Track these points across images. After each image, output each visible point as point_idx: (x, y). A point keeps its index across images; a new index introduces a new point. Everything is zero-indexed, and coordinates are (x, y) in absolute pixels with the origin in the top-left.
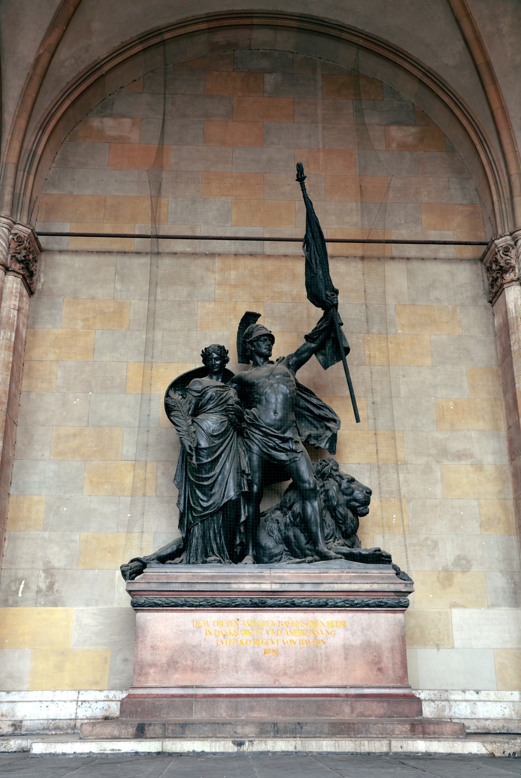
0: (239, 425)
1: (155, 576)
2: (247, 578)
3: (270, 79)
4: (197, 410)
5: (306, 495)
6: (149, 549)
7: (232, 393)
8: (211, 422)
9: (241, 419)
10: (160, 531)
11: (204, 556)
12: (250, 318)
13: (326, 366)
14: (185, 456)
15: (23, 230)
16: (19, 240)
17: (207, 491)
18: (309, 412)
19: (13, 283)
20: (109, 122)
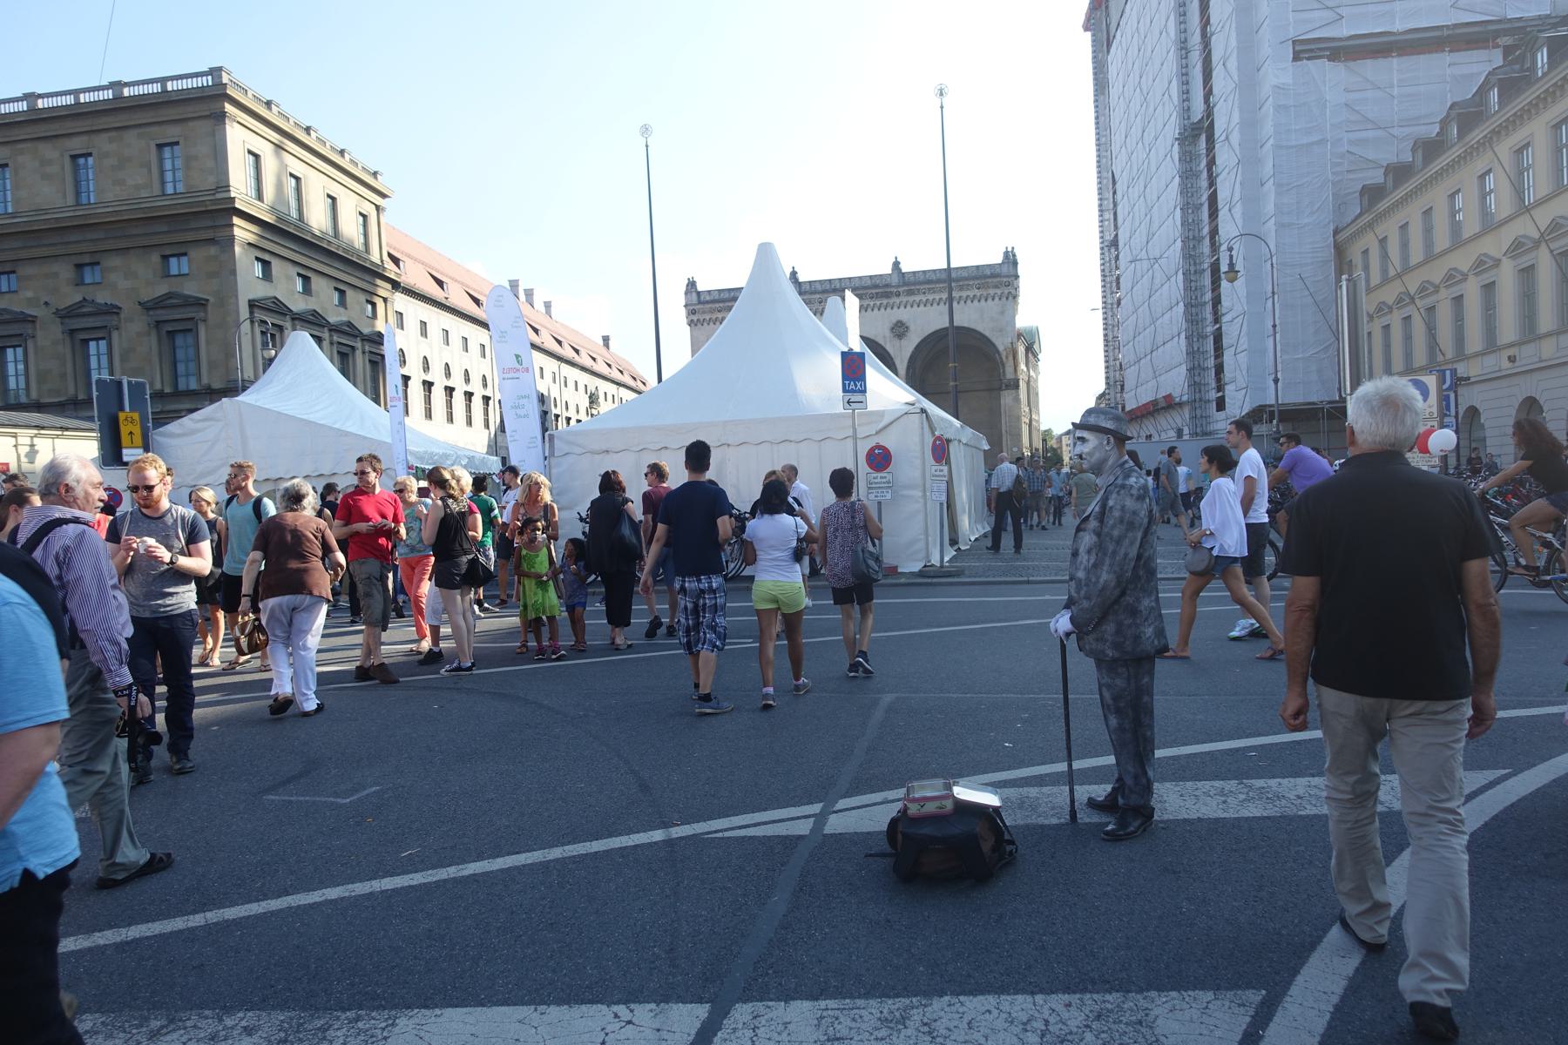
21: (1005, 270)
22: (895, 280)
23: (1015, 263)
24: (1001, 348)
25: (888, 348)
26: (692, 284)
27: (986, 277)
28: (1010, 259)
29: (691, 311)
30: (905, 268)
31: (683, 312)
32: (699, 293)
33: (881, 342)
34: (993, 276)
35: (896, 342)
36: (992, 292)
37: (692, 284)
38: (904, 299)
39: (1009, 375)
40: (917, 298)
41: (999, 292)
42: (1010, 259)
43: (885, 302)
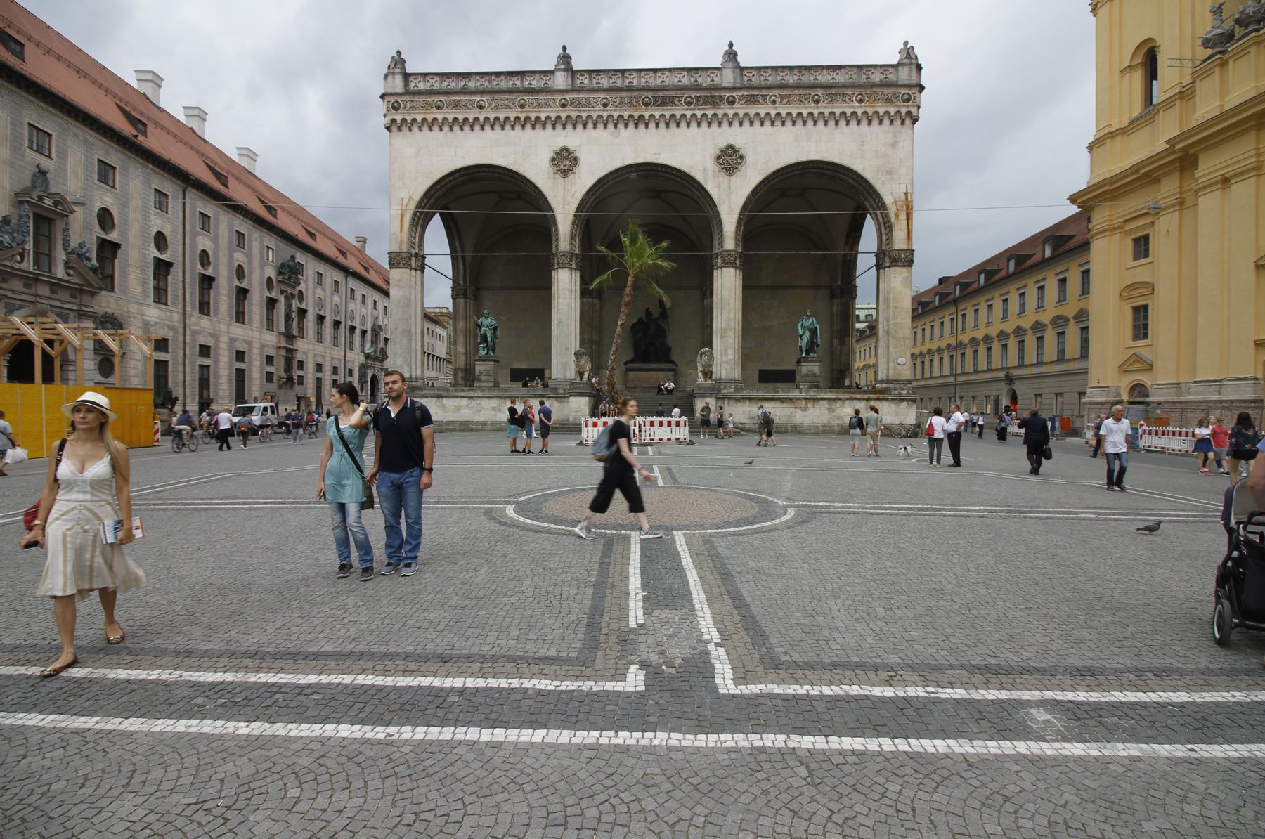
1: (630, 365)
2: (646, 366)
19: (597, 301)
21: (904, 75)
22: (728, 78)
23: (919, 68)
24: (888, 200)
25: (711, 187)
26: (398, 61)
27: (873, 85)
28: (909, 58)
30: (744, 61)
31: (381, 106)
32: (406, 76)
34: (884, 84)
35: (723, 178)
37: (398, 61)
39: (899, 243)
42: (909, 58)
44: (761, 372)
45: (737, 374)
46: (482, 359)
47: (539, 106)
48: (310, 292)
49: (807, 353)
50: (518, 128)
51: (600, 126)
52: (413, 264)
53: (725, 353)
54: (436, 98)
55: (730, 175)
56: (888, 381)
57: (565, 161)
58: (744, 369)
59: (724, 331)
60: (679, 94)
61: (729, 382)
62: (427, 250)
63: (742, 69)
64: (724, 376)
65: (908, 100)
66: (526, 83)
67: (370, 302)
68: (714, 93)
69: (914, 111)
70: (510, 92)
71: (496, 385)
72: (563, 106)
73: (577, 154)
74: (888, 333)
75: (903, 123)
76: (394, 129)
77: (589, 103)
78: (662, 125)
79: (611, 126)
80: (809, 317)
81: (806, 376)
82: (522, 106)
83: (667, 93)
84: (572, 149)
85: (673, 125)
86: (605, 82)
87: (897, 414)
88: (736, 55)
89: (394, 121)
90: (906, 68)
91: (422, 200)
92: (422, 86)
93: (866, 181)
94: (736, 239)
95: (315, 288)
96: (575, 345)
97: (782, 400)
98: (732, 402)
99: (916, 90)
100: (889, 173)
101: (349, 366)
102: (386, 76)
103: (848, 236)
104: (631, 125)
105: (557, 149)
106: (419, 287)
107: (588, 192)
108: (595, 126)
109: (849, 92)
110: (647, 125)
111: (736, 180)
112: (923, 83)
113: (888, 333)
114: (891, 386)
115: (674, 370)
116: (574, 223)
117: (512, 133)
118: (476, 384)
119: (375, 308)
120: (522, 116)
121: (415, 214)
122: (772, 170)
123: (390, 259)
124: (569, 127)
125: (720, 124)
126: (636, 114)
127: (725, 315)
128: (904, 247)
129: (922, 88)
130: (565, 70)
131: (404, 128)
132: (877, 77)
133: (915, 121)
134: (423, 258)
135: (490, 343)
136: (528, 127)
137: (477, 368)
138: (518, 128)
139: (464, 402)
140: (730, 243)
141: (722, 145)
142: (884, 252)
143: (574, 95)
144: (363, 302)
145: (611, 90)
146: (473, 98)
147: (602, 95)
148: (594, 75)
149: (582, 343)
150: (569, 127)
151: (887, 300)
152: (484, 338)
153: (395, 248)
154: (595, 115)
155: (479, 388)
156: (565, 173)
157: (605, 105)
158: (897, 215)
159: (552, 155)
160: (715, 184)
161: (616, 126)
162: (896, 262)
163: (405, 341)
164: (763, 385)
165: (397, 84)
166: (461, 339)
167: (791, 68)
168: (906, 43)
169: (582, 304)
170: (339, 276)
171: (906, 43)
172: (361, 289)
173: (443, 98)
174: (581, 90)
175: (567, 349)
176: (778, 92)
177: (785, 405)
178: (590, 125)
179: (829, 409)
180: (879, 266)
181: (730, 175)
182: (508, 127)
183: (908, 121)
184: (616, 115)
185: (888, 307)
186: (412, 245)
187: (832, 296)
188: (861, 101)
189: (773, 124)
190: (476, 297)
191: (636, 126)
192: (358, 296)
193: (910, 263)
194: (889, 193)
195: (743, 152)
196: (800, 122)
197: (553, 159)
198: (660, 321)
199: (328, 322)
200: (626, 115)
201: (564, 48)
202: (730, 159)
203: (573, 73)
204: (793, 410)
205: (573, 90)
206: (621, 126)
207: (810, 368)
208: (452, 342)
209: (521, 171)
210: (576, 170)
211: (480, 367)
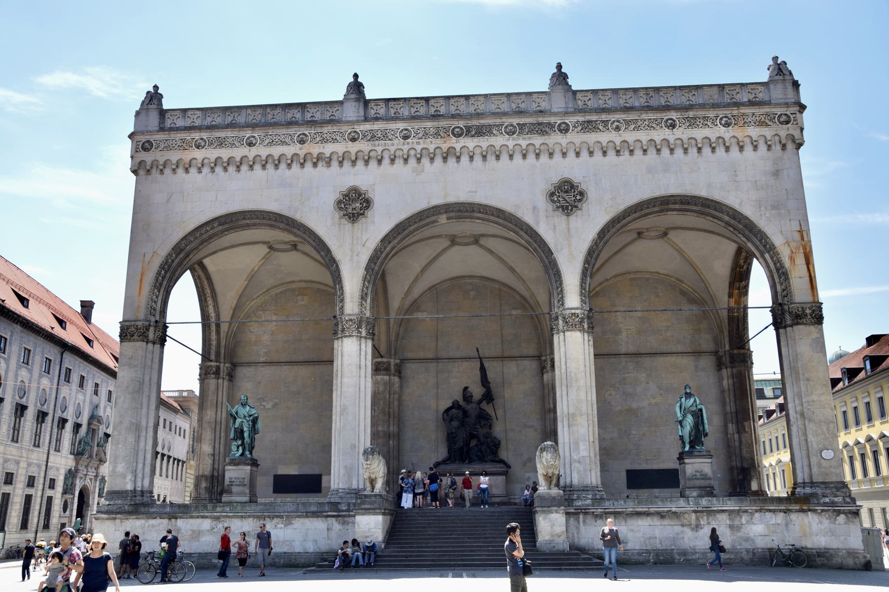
0: (463, 424)
3: (472, 293)
4: (451, 420)
5: (482, 444)
6: (440, 459)
7: (461, 413)
8: (455, 424)
9: (463, 422)
10: (442, 453)
11: (454, 461)
12: (466, 389)
13: (488, 403)
14: (448, 434)
15: (398, 361)
16: (396, 364)
17: (455, 444)
18: (485, 419)
19: (396, 379)
20: (420, 314)
23: (796, 85)
24: (778, 240)
25: (544, 230)
26: (154, 97)
29: (141, 143)
31: (127, 146)
32: (163, 113)
33: (528, 219)
35: (560, 219)
36: (754, 132)
37: (154, 97)
38: (576, 137)
39: (800, 294)
40: (604, 137)
41: (768, 132)
43: (537, 140)
44: (629, 472)
45: (594, 478)
46: (234, 462)
47: (324, 141)
48: (11, 375)
49: (692, 447)
50: (295, 167)
51: (399, 162)
52: (151, 335)
53: (576, 450)
54: (196, 135)
55: (568, 215)
56: (812, 484)
57: (354, 205)
58: (604, 468)
59: (571, 417)
60: (498, 121)
61: (585, 489)
62: (169, 319)
63: (575, 93)
64: (575, 481)
65: (787, 122)
66: (308, 116)
67: (89, 387)
68: (541, 120)
69: (796, 134)
70: (290, 124)
71: (253, 500)
72: (353, 140)
73: (370, 195)
74: (802, 415)
75: (784, 147)
76: (142, 172)
77: (385, 137)
78: (478, 159)
79: (412, 161)
80: (688, 395)
81: (693, 478)
82: (302, 142)
83: (482, 122)
84: (363, 188)
85: (491, 158)
86: (405, 112)
87: (832, 533)
88: (565, 77)
89: (141, 163)
90: (780, 86)
91: (169, 255)
92: (180, 123)
93: (746, 218)
94: (581, 294)
95: (19, 367)
96: (365, 441)
97: (661, 515)
98: (589, 519)
99: (796, 109)
100: (776, 207)
101: (51, 474)
102: (138, 114)
103: (731, 285)
104: (439, 160)
105: (344, 189)
106: (156, 366)
107: (382, 241)
108: (393, 161)
109: (711, 114)
110: (458, 158)
111: (576, 220)
112: (803, 101)
113: (802, 415)
114: (819, 491)
115: (505, 474)
116: (365, 279)
117: (288, 173)
118: (225, 498)
119: (96, 393)
120: (302, 153)
121: (159, 273)
122: (622, 207)
123: (122, 328)
124: (360, 164)
125: (551, 155)
126: (445, 147)
127: (573, 395)
128: (810, 299)
129: (803, 107)
130: (357, 100)
131: (154, 171)
132: (745, 97)
133: (799, 145)
134: (165, 327)
135: (247, 439)
136: (309, 165)
137: (228, 475)
138: (295, 167)
139: (206, 524)
140: (573, 300)
141: (556, 179)
142: (780, 305)
143: (367, 127)
144: (81, 385)
145: (413, 118)
146: (242, 134)
147: (401, 125)
148: (391, 104)
149: (375, 435)
150: (360, 164)
151: (795, 370)
152: (240, 433)
153: (130, 317)
154: (392, 149)
155: (230, 503)
156: (354, 217)
157: (406, 138)
158: (792, 259)
159: (337, 196)
160: (549, 227)
161: (419, 160)
162: (798, 318)
163: (131, 439)
164: (633, 493)
165: (153, 120)
166: (208, 435)
167: (635, 90)
168: (775, 59)
169: (375, 383)
170: (53, 352)
171: (775, 59)
172: (79, 368)
173: (205, 135)
174: (377, 119)
175: (353, 447)
176: (621, 116)
177: (666, 522)
178: (386, 161)
179: (731, 527)
180: (778, 323)
181: (568, 215)
182: (283, 166)
183: (790, 146)
184: (418, 148)
185: (798, 379)
186: (152, 310)
187: (720, 366)
188: (727, 125)
189: (618, 152)
190: (231, 376)
191: (445, 159)
192: (75, 378)
193: (818, 319)
194: (778, 234)
195: (583, 187)
196: (652, 151)
197: (339, 202)
198: (484, 405)
199: (30, 415)
200: (432, 148)
201: (356, 76)
202: (567, 197)
203: (367, 103)
204: (678, 529)
205: (366, 119)
206: (425, 161)
207: (697, 467)
208: (197, 439)
209: (298, 217)
210: (369, 213)
211: (232, 473)
